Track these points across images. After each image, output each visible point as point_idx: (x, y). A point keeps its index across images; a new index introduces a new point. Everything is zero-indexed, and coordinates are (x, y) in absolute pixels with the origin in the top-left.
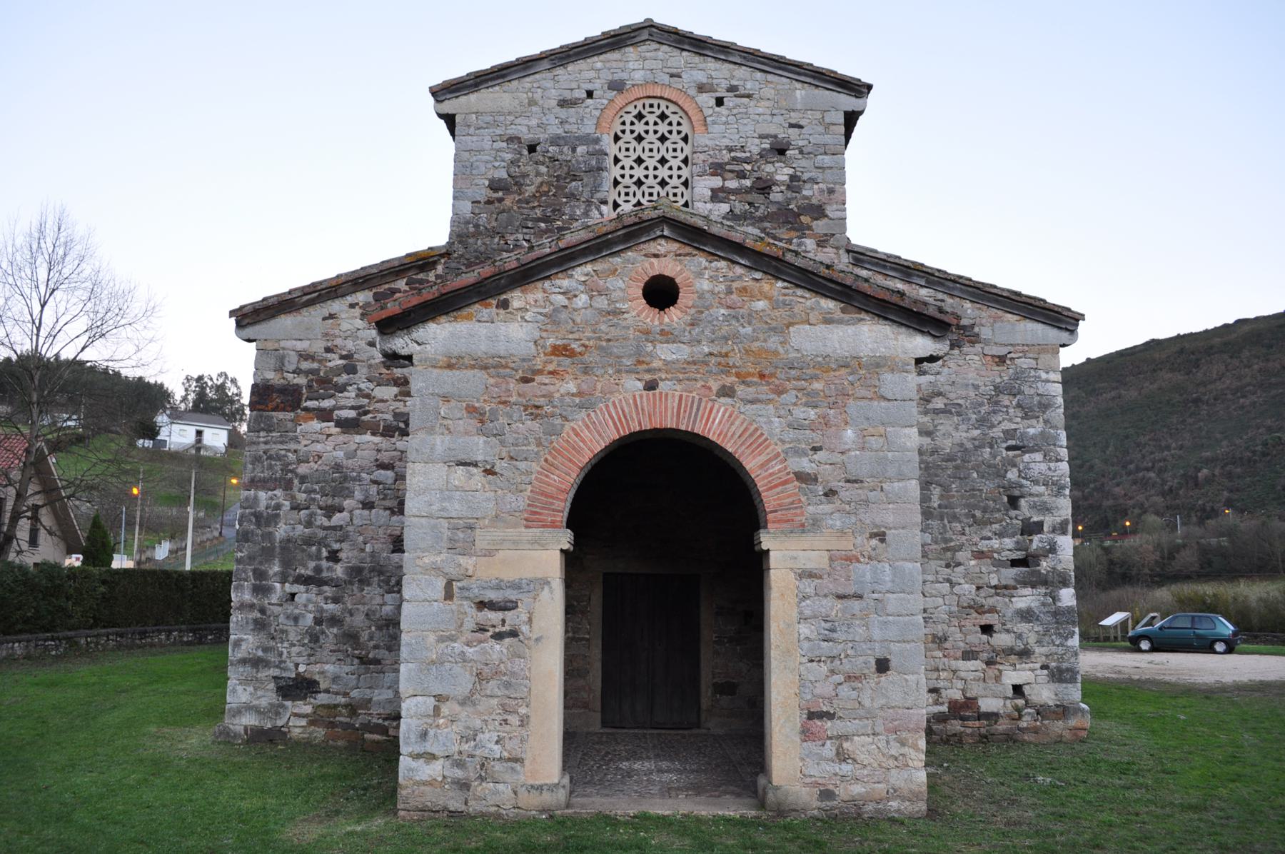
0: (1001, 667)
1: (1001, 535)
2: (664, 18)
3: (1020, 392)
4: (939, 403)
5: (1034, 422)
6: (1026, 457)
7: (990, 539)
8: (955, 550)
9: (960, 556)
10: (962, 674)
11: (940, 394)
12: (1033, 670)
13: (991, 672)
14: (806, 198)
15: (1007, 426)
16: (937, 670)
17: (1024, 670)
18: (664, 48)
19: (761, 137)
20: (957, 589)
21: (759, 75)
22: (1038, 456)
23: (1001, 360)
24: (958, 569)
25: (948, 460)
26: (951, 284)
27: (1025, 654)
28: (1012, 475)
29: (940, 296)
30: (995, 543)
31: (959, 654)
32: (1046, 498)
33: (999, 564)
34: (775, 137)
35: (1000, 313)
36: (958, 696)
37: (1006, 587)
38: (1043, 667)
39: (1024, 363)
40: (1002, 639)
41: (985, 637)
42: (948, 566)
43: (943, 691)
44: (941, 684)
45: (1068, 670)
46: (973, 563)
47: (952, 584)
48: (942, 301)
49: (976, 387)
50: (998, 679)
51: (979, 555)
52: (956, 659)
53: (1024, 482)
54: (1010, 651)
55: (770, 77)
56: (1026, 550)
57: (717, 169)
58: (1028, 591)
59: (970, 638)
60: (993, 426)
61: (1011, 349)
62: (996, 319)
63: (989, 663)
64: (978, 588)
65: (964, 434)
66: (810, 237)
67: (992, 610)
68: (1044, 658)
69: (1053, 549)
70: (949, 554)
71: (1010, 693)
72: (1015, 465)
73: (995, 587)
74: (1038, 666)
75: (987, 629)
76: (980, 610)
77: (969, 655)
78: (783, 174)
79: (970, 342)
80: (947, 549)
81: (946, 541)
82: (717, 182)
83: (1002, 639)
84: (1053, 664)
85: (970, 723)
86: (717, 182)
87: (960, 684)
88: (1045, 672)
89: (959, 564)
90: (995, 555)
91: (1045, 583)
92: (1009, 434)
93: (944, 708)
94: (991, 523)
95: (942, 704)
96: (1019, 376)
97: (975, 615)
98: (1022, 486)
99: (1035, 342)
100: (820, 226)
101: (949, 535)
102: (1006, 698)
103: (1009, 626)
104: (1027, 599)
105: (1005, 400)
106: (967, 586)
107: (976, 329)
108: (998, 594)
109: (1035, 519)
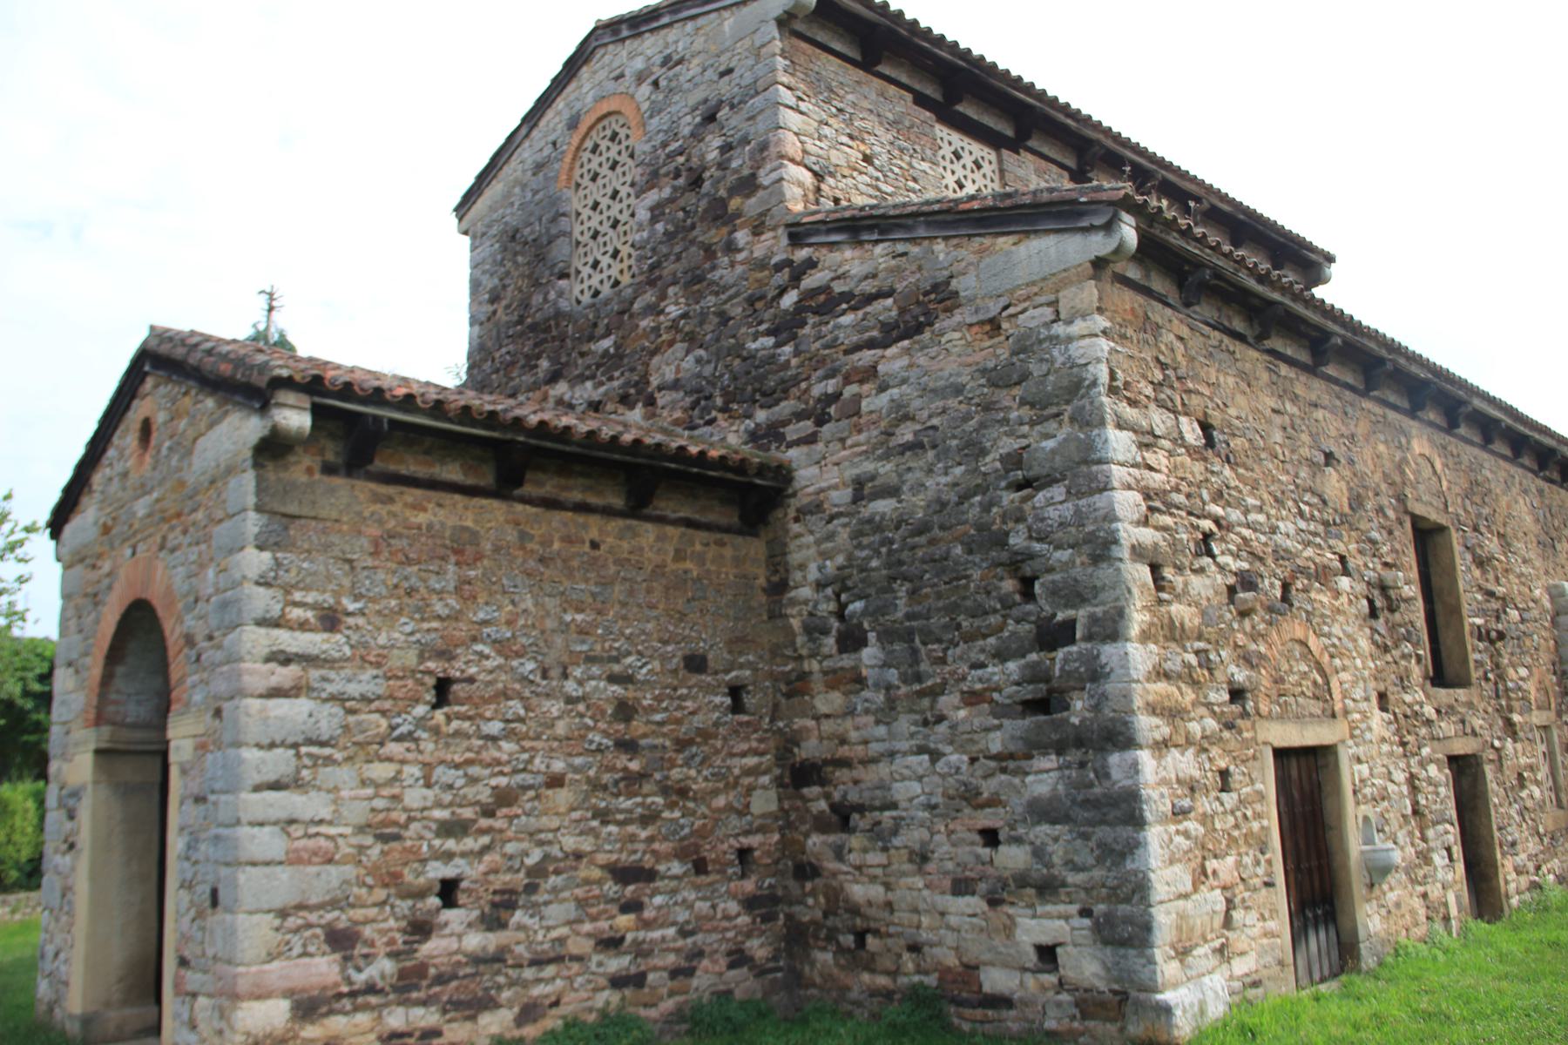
0: (1011, 911)
1: (1001, 656)
2: (607, 14)
3: (1025, 377)
4: (906, 434)
5: (1052, 426)
6: (1040, 497)
7: (983, 666)
8: (934, 693)
9: (947, 702)
10: (953, 920)
11: (908, 417)
12: (1067, 918)
13: (998, 917)
14: (736, 171)
15: (1008, 445)
16: (916, 911)
17: (1049, 916)
18: (611, 47)
19: (695, 109)
20: (941, 766)
21: (690, 26)
22: (1058, 492)
23: (994, 326)
24: (942, 728)
25: (920, 533)
26: (910, 222)
27: (1047, 888)
28: (1017, 540)
29: (900, 248)
30: (993, 670)
31: (947, 883)
32: (1077, 572)
33: (1000, 711)
34: (706, 101)
35: (987, 241)
36: (951, 960)
37: (1012, 756)
38: (1085, 912)
39: (1034, 317)
40: (1012, 857)
41: (985, 852)
42: (926, 723)
43: (926, 949)
44: (924, 935)
45: (1128, 920)
46: (962, 713)
47: (935, 756)
48: (904, 254)
49: (958, 390)
50: (1009, 929)
51: (972, 699)
52: (943, 893)
53: (1037, 546)
54: (1022, 881)
55: (701, 21)
56: (1048, 680)
57: (653, 180)
58: (1050, 761)
59: (964, 853)
60: (984, 452)
61: (1003, 301)
62: (981, 252)
63: (994, 902)
64: (973, 760)
65: (943, 480)
66: (742, 226)
67: (994, 802)
68: (1083, 895)
69: (1096, 674)
70: (926, 702)
71: (1032, 958)
72: (1020, 519)
73: (997, 757)
74: (1074, 909)
75: (990, 837)
76: (971, 797)
77: (961, 887)
78: (711, 148)
79: (946, 310)
80: (921, 694)
81: (918, 678)
82: (653, 197)
83: (1012, 857)
84: (1100, 908)
85: (968, 1012)
86: (653, 197)
87: (950, 938)
88: (1087, 922)
89: (941, 719)
90: (996, 696)
91: (1079, 742)
92: (1014, 460)
93: (931, 980)
94: (985, 637)
95: (926, 973)
96: (1025, 346)
97: (967, 811)
98: (1031, 556)
99: (1047, 270)
100: (752, 206)
101: (924, 667)
102: (1024, 970)
103: (1021, 831)
104: (1044, 778)
105: (1006, 398)
106: (954, 758)
107: (954, 282)
108: (1004, 770)
109: (1060, 616)
